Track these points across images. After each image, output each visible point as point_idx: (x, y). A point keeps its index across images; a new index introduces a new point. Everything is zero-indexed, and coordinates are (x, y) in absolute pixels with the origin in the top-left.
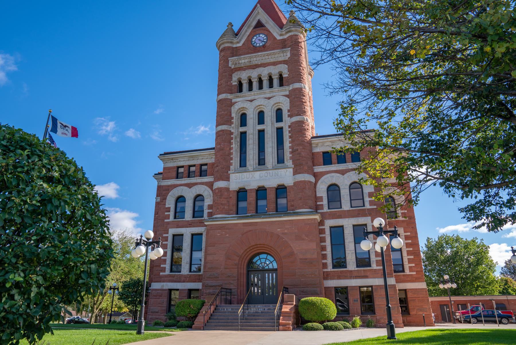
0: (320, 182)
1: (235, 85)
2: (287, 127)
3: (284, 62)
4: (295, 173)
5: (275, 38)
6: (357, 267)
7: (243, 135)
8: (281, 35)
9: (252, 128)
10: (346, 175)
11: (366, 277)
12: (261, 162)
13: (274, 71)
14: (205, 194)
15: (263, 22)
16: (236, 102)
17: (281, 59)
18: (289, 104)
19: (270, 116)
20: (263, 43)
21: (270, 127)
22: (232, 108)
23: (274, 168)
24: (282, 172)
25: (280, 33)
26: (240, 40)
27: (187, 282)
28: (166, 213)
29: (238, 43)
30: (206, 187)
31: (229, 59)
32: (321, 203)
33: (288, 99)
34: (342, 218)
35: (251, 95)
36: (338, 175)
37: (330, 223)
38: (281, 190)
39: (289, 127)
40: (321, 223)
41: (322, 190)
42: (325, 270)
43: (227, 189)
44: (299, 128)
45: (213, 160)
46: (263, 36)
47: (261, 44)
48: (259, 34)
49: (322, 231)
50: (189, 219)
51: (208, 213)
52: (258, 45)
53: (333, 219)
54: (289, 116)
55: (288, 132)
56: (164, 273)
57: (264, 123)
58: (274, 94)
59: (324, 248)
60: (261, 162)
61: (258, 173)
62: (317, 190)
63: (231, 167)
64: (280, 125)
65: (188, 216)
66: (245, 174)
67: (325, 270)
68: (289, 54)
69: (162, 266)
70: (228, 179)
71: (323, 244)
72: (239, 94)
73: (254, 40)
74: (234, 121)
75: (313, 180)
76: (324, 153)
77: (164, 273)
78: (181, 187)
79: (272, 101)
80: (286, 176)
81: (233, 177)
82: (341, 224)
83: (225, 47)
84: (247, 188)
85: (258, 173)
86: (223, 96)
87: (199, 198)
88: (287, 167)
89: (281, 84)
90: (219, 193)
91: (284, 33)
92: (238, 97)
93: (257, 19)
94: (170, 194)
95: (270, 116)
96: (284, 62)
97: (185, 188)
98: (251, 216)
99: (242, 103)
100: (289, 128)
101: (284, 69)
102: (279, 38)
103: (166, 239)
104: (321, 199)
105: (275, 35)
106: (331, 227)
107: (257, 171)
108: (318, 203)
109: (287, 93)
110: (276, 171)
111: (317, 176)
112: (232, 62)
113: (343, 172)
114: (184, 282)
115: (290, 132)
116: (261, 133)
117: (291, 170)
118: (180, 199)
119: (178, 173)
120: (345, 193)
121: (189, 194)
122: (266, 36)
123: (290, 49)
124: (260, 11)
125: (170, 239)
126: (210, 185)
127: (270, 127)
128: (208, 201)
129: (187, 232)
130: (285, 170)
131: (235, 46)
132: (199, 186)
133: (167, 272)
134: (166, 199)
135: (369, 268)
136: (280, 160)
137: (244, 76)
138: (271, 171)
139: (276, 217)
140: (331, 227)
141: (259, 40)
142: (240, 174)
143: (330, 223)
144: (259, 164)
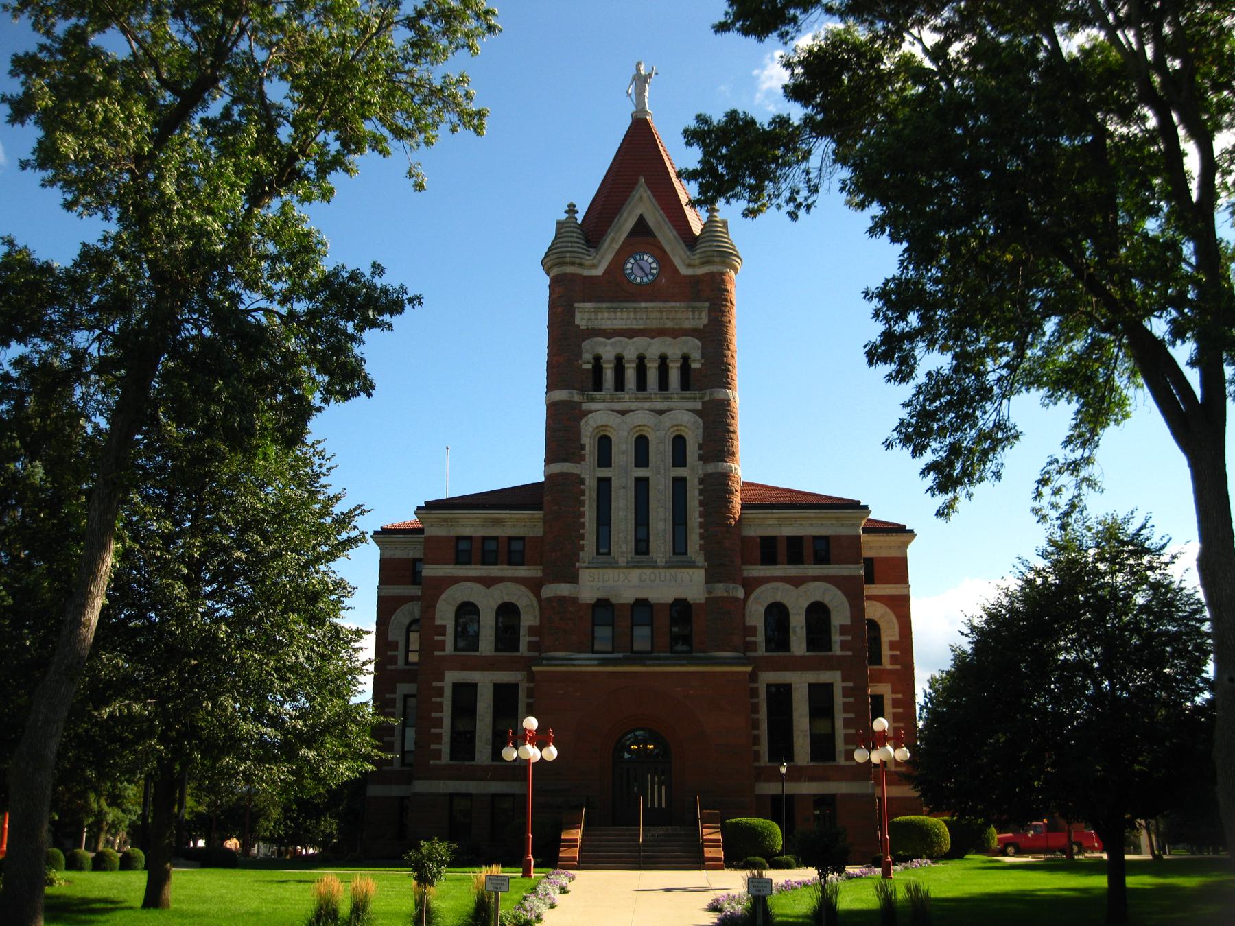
0: (752, 597)
1: (587, 370)
2: (696, 481)
3: (693, 332)
4: (710, 579)
5: (676, 271)
6: (812, 760)
7: (604, 485)
8: (689, 266)
9: (622, 471)
10: (802, 588)
11: (825, 778)
12: (642, 546)
13: (674, 349)
14: (521, 604)
15: (651, 222)
16: (591, 412)
17: (688, 324)
18: (701, 430)
19: (660, 451)
20: (651, 277)
21: (661, 476)
22: (583, 422)
23: (669, 565)
24: (684, 574)
25: (687, 262)
26: (600, 262)
27: (491, 779)
28: (437, 638)
29: (594, 266)
30: (523, 588)
31: (576, 305)
32: (753, 639)
33: (700, 421)
34: (788, 670)
35: (626, 402)
36: (788, 586)
37: (770, 677)
38: (681, 608)
39: (701, 481)
40: (753, 677)
41: (756, 614)
42: (757, 764)
43: (574, 600)
44: (718, 485)
45: (539, 531)
46: (650, 260)
47: (645, 280)
48: (642, 254)
49: (754, 693)
50: (805, 764)
51: (529, 642)
52: (638, 280)
53: (774, 670)
54: (700, 458)
55: (697, 493)
56: (438, 762)
57: (647, 466)
58: (672, 404)
59: (755, 725)
60: (642, 546)
61: (636, 573)
62: (747, 613)
63: (581, 554)
64: (680, 472)
65: (487, 645)
66: (610, 572)
67: (757, 764)
68: (705, 320)
69: (433, 747)
70: (574, 579)
71: (754, 716)
72: (596, 394)
73: (629, 266)
74: (587, 452)
75: (741, 594)
76: (763, 539)
77: (438, 762)
78: (469, 584)
79: (666, 420)
80: (690, 585)
81: (585, 575)
82: (787, 681)
83: (565, 275)
84: (614, 601)
85: (636, 572)
86: (561, 395)
87: (508, 611)
88: (691, 565)
89: (685, 385)
90: (555, 609)
91: (697, 262)
92: (592, 400)
93: (638, 212)
94: (443, 596)
95: (660, 451)
96: (693, 332)
97: (478, 587)
98: (625, 658)
99: (601, 414)
100: (700, 483)
101: (693, 347)
102: (684, 271)
103: (440, 693)
104: (752, 630)
105: (677, 262)
106: (769, 686)
107: (634, 567)
108: (748, 639)
109: (699, 406)
110: (673, 571)
111: (750, 585)
112: (584, 315)
113: (797, 582)
114: (480, 779)
115: (701, 492)
116: (642, 485)
117: (702, 572)
118: (467, 610)
119: (457, 552)
120: (798, 621)
121: (488, 602)
122: (657, 260)
123: (707, 304)
124: (645, 196)
125: (448, 692)
126: (534, 586)
127: (661, 476)
128: (529, 619)
129: (485, 681)
130: (690, 571)
131: (586, 273)
132: (509, 584)
133: (445, 759)
134: (435, 607)
135: (831, 764)
136: (679, 547)
137: (608, 350)
138: (662, 571)
139: (674, 665)
140: (769, 686)
141: (642, 268)
142: (601, 571)
143: (770, 677)
144: (637, 552)
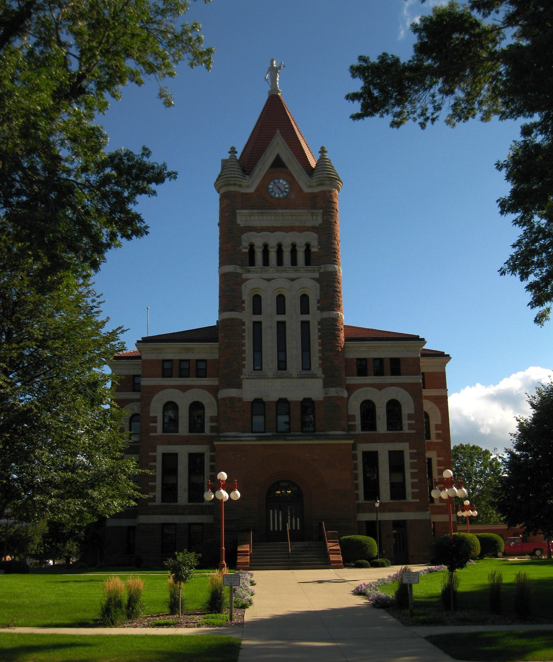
0: (352, 396)
4: (326, 385)
5: (301, 190)
6: (391, 499)
7: (257, 325)
8: (309, 187)
9: (269, 317)
10: (383, 391)
11: (400, 510)
12: (282, 365)
13: (300, 239)
17: (309, 224)
18: (319, 291)
19: (293, 304)
20: (285, 194)
21: (293, 319)
22: (243, 286)
23: (301, 377)
27: (187, 514)
28: (152, 424)
29: (249, 187)
31: (237, 211)
33: (318, 285)
38: (307, 404)
39: (319, 323)
40: (354, 447)
41: (354, 408)
42: (357, 502)
43: (240, 400)
44: (331, 326)
45: (216, 356)
46: (284, 183)
47: (281, 195)
48: (279, 178)
49: (355, 457)
50: (387, 501)
51: (211, 427)
52: (277, 196)
54: (319, 308)
55: (317, 331)
56: (153, 504)
59: (356, 477)
60: (282, 365)
61: (278, 382)
63: (244, 370)
64: (305, 318)
67: (357, 502)
70: (239, 386)
73: (271, 186)
75: (345, 394)
77: (153, 504)
78: (171, 390)
80: (314, 389)
81: (246, 383)
84: (265, 400)
86: (229, 268)
87: (196, 407)
88: (314, 376)
89: (308, 262)
92: (249, 271)
94: (155, 398)
95: (293, 304)
96: (313, 229)
97: (177, 391)
99: (254, 281)
100: (319, 324)
101: (313, 238)
102: (306, 190)
103: (154, 459)
104: (353, 418)
105: (301, 184)
108: (350, 423)
109: (317, 275)
110: (302, 380)
111: (351, 389)
112: (244, 218)
115: (319, 330)
116: (281, 325)
117: (321, 381)
119: (163, 369)
121: (184, 402)
122: (289, 183)
123: (321, 211)
125: (159, 459)
126: (214, 390)
127: (293, 319)
128: (210, 411)
129: (183, 452)
130: (314, 380)
131: (243, 191)
132: (196, 390)
133: (158, 502)
134: (149, 404)
135: (403, 501)
136: (306, 365)
137: (258, 240)
139: (305, 440)
141: (279, 187)
144: (279, 369)
